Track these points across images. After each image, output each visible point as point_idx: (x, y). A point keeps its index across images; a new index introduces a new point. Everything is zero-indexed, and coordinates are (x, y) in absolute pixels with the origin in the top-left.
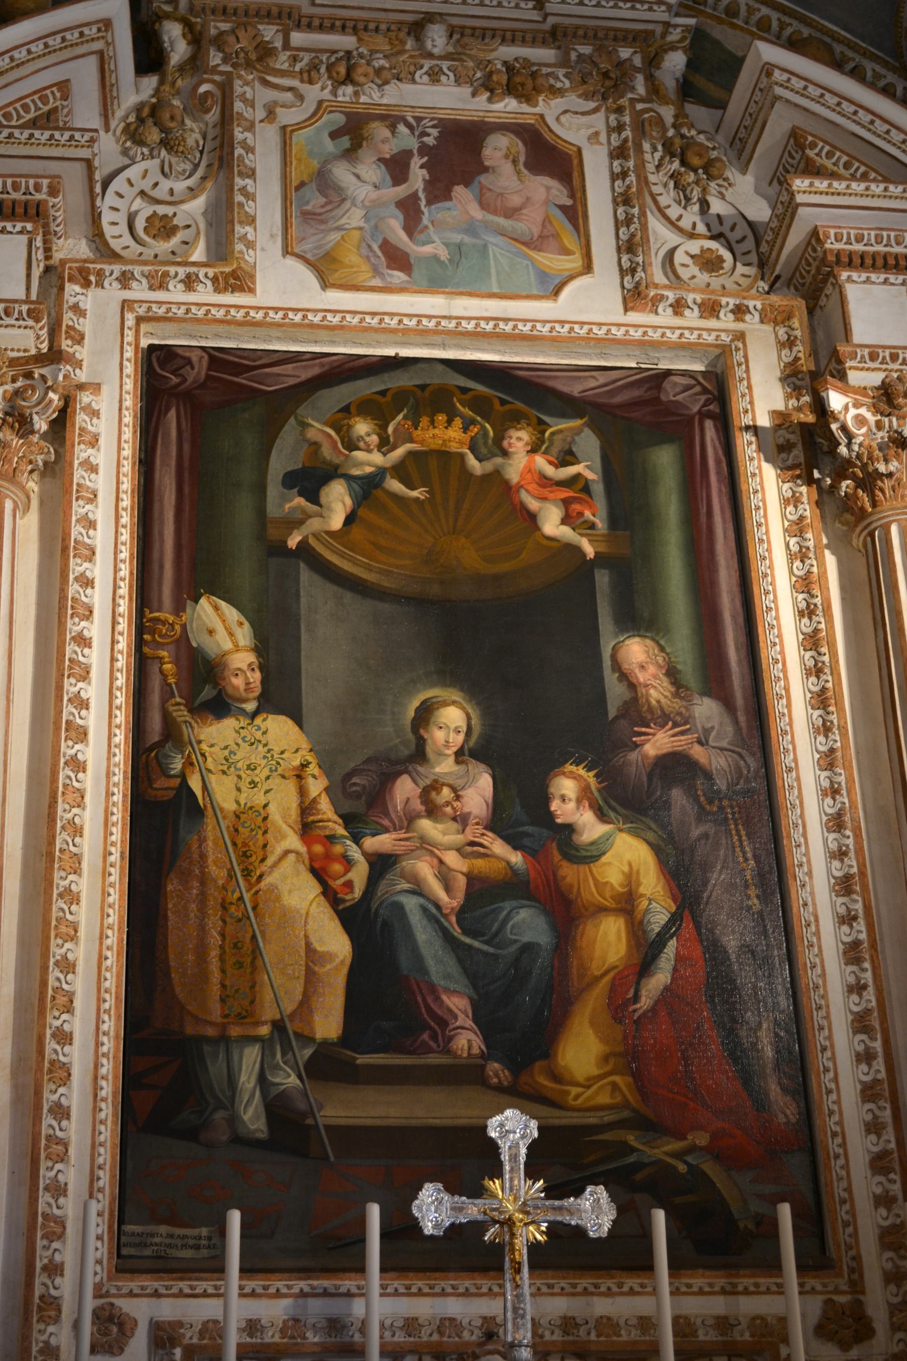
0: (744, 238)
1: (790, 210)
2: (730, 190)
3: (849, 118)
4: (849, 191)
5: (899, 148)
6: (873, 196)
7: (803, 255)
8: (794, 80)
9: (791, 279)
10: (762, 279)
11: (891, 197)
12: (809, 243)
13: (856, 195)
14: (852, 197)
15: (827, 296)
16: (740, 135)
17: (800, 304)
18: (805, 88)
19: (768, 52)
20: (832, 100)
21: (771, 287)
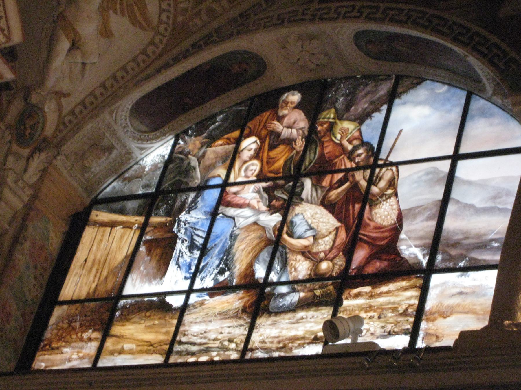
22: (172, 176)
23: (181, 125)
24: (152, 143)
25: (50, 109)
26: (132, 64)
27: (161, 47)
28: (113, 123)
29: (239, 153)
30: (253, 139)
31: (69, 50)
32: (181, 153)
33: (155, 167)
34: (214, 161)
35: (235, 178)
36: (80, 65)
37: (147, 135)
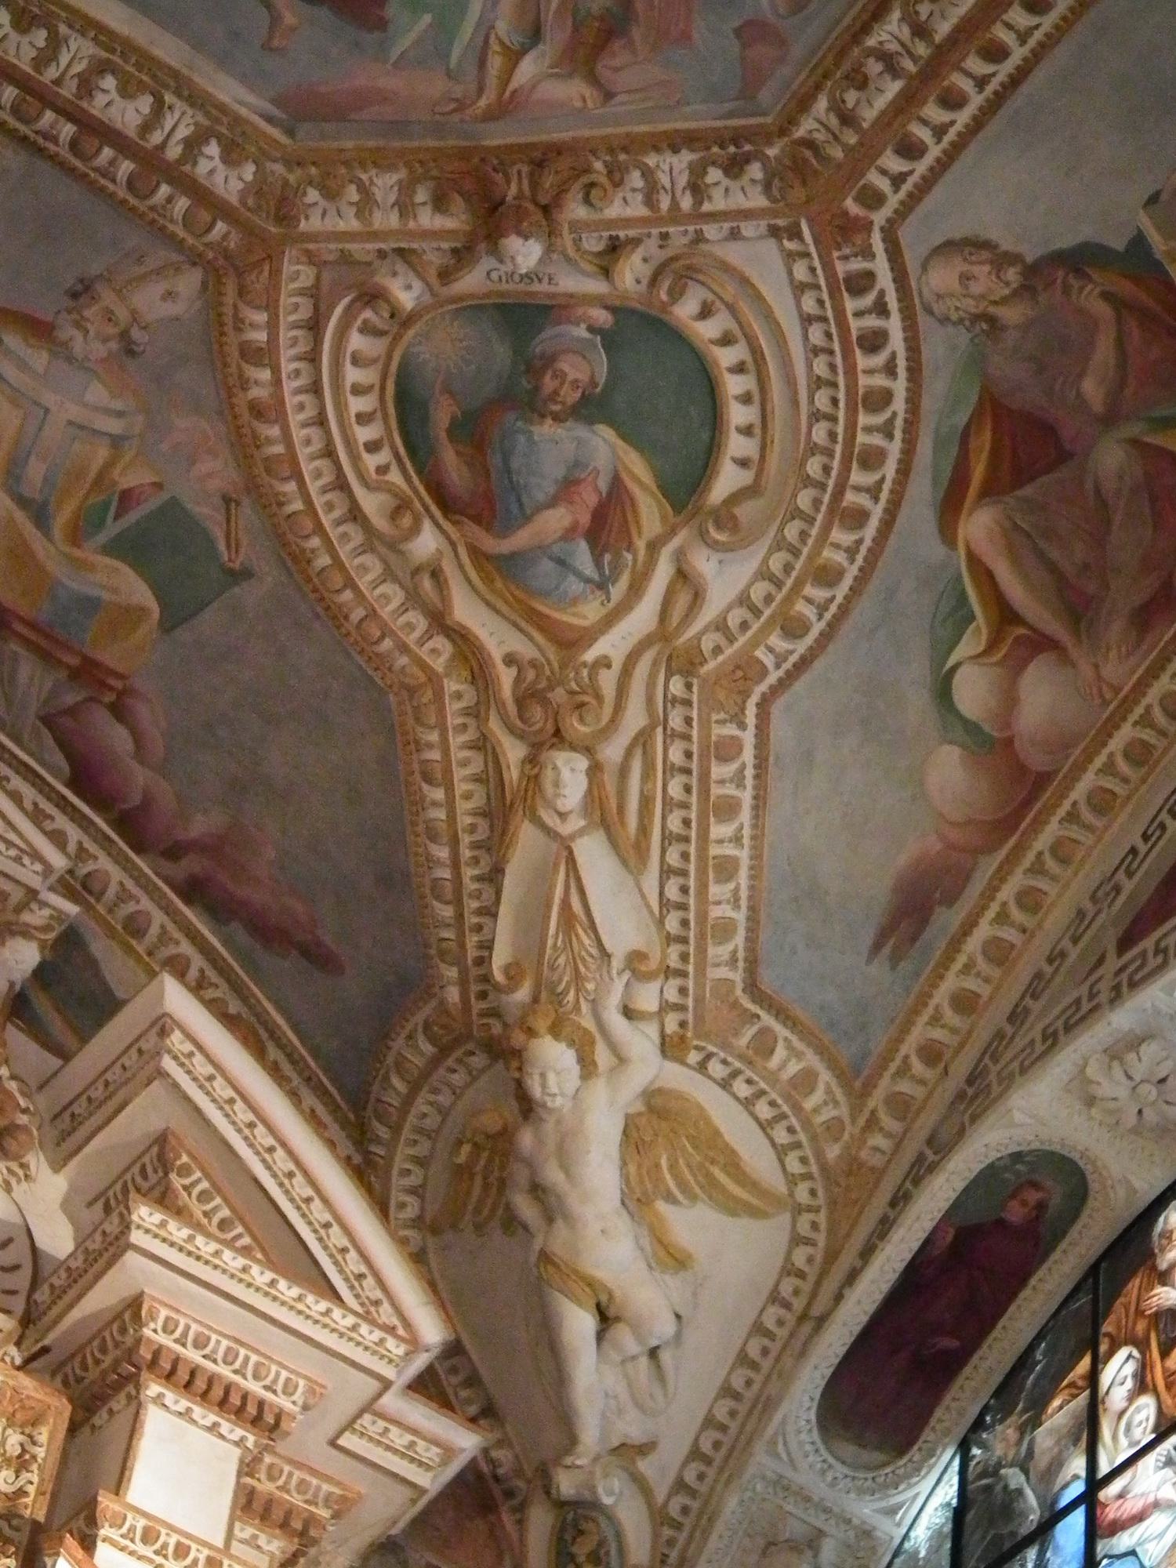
0: (16, 1267)
1: (112, 1250)
2: (24, 1185)
3: (258, 1153)
4: (217, 1261)
5: (315, 1231)
6: (249, 1285)
7: (100, 1331)
8: (198, 1058)
9: (63, 1364)
10: (18, 1344)
11: (275, 1298)
12: (119, 1316)
13: (224, 1271)
14: (218, 1272)
15: (111, 1412)
16: (76, 1109)
17: (60, 1409)
18: (211, 1078)
19: (176, 999)
20: (243, 1115)
21: (28, 1361)
22: (977, 1536)
23: (961, 1413)
24: (910, 1486)
25: (614, 1492)
26: (773, 1312)
27: (821, 1239)
28: (789, 1473)
29: (1103, 1402)
30: (1123, 1353)
31: (600, 1336)
32: (981, 1476)
33: (937, 1536)
34: (1056, 1450)
35: (1111, 1462)
36: (644, 1362)
37: (888, 1470)
